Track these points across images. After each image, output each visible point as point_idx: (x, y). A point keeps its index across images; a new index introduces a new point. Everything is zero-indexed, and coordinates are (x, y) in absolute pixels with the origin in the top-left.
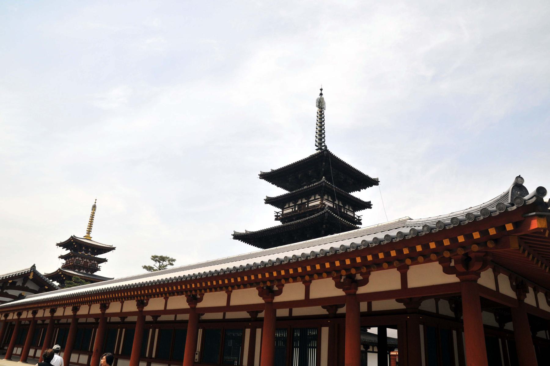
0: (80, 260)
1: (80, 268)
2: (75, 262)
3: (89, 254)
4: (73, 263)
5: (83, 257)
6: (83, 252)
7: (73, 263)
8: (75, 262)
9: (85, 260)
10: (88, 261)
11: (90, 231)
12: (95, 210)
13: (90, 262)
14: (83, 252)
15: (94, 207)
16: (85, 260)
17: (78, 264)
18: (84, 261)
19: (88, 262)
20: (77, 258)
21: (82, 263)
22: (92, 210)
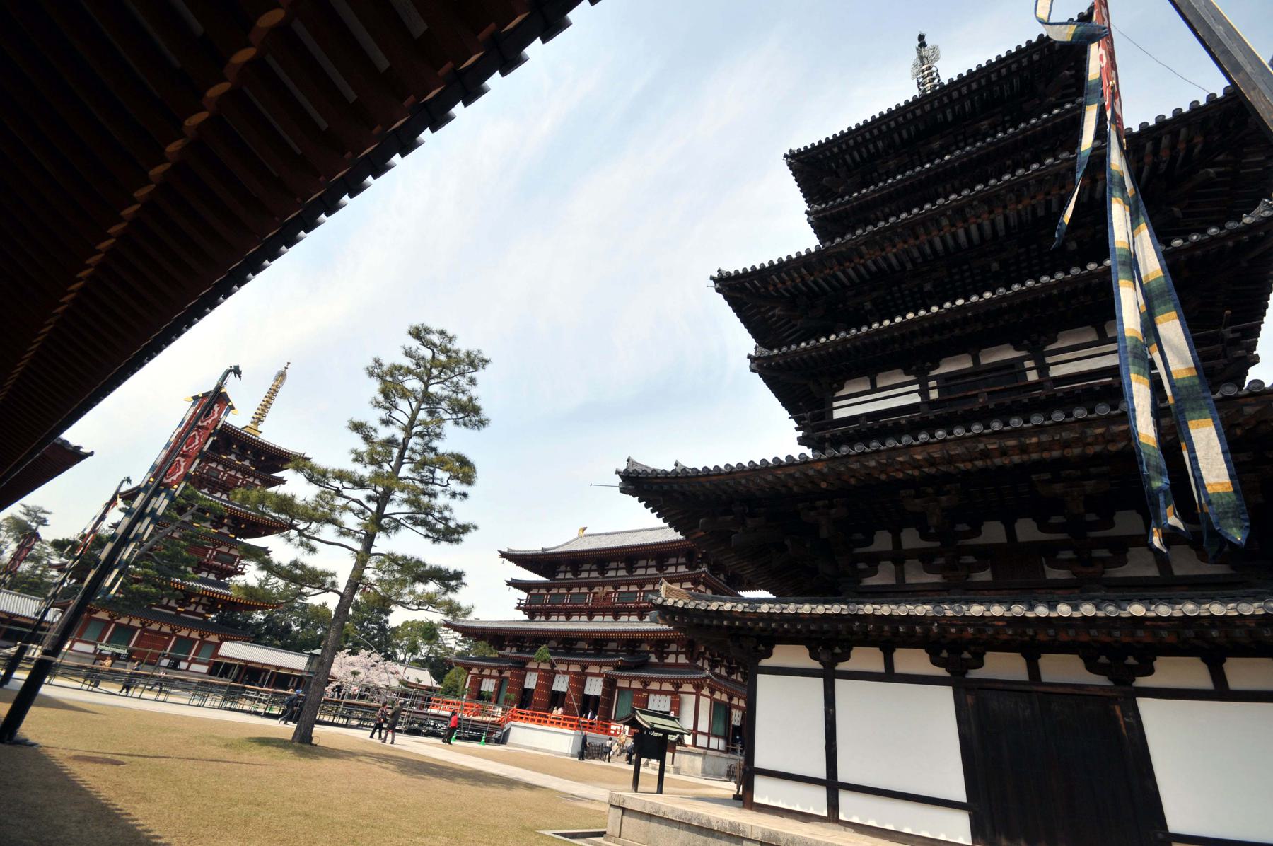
0: (220, 471)
1: (214, 486)
2: (205, 471)
3: (247, 463)
4: (200, 473)
5: (228, 465)
6: (232, 457)
7: (200, 473)
8: (205, 471)
9: (232, 473)
10: (239, 475)
11: (259, 420)
12: (281, 382)
13: (243, 480)
14: (232, 457)
15: (282, 376)
16: (232, 473)
17: (211, 476)
18: (230, 475)
19: (238, 478)
20: (214, 465)
21: (222, 477)
22: (276, 380)
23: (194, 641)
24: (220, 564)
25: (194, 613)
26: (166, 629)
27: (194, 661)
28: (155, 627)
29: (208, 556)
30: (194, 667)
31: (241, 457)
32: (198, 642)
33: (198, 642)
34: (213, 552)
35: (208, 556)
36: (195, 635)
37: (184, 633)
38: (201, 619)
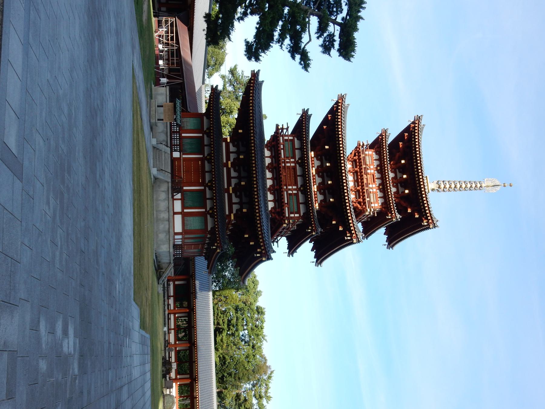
14: (391, 175)
23: (205, 207)
24: (286, 202)
25: (231, 204)
26: (207, 177)
27: (184, 215)
28: (207, 167)
29: (290, 187)
30: (178, 219)
31: (397, 182)
32: (204, 210)
33: (204, 210)
34: (295, 190)
35: (290, 187)
36: (209, 204)
37: (208, 194)
38: (227, 213)
